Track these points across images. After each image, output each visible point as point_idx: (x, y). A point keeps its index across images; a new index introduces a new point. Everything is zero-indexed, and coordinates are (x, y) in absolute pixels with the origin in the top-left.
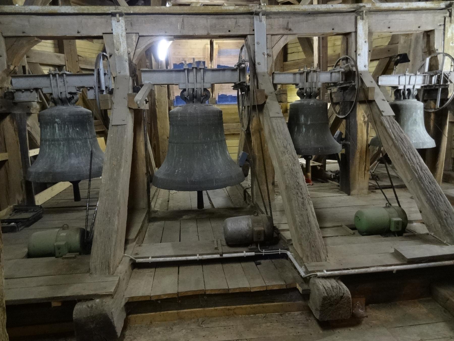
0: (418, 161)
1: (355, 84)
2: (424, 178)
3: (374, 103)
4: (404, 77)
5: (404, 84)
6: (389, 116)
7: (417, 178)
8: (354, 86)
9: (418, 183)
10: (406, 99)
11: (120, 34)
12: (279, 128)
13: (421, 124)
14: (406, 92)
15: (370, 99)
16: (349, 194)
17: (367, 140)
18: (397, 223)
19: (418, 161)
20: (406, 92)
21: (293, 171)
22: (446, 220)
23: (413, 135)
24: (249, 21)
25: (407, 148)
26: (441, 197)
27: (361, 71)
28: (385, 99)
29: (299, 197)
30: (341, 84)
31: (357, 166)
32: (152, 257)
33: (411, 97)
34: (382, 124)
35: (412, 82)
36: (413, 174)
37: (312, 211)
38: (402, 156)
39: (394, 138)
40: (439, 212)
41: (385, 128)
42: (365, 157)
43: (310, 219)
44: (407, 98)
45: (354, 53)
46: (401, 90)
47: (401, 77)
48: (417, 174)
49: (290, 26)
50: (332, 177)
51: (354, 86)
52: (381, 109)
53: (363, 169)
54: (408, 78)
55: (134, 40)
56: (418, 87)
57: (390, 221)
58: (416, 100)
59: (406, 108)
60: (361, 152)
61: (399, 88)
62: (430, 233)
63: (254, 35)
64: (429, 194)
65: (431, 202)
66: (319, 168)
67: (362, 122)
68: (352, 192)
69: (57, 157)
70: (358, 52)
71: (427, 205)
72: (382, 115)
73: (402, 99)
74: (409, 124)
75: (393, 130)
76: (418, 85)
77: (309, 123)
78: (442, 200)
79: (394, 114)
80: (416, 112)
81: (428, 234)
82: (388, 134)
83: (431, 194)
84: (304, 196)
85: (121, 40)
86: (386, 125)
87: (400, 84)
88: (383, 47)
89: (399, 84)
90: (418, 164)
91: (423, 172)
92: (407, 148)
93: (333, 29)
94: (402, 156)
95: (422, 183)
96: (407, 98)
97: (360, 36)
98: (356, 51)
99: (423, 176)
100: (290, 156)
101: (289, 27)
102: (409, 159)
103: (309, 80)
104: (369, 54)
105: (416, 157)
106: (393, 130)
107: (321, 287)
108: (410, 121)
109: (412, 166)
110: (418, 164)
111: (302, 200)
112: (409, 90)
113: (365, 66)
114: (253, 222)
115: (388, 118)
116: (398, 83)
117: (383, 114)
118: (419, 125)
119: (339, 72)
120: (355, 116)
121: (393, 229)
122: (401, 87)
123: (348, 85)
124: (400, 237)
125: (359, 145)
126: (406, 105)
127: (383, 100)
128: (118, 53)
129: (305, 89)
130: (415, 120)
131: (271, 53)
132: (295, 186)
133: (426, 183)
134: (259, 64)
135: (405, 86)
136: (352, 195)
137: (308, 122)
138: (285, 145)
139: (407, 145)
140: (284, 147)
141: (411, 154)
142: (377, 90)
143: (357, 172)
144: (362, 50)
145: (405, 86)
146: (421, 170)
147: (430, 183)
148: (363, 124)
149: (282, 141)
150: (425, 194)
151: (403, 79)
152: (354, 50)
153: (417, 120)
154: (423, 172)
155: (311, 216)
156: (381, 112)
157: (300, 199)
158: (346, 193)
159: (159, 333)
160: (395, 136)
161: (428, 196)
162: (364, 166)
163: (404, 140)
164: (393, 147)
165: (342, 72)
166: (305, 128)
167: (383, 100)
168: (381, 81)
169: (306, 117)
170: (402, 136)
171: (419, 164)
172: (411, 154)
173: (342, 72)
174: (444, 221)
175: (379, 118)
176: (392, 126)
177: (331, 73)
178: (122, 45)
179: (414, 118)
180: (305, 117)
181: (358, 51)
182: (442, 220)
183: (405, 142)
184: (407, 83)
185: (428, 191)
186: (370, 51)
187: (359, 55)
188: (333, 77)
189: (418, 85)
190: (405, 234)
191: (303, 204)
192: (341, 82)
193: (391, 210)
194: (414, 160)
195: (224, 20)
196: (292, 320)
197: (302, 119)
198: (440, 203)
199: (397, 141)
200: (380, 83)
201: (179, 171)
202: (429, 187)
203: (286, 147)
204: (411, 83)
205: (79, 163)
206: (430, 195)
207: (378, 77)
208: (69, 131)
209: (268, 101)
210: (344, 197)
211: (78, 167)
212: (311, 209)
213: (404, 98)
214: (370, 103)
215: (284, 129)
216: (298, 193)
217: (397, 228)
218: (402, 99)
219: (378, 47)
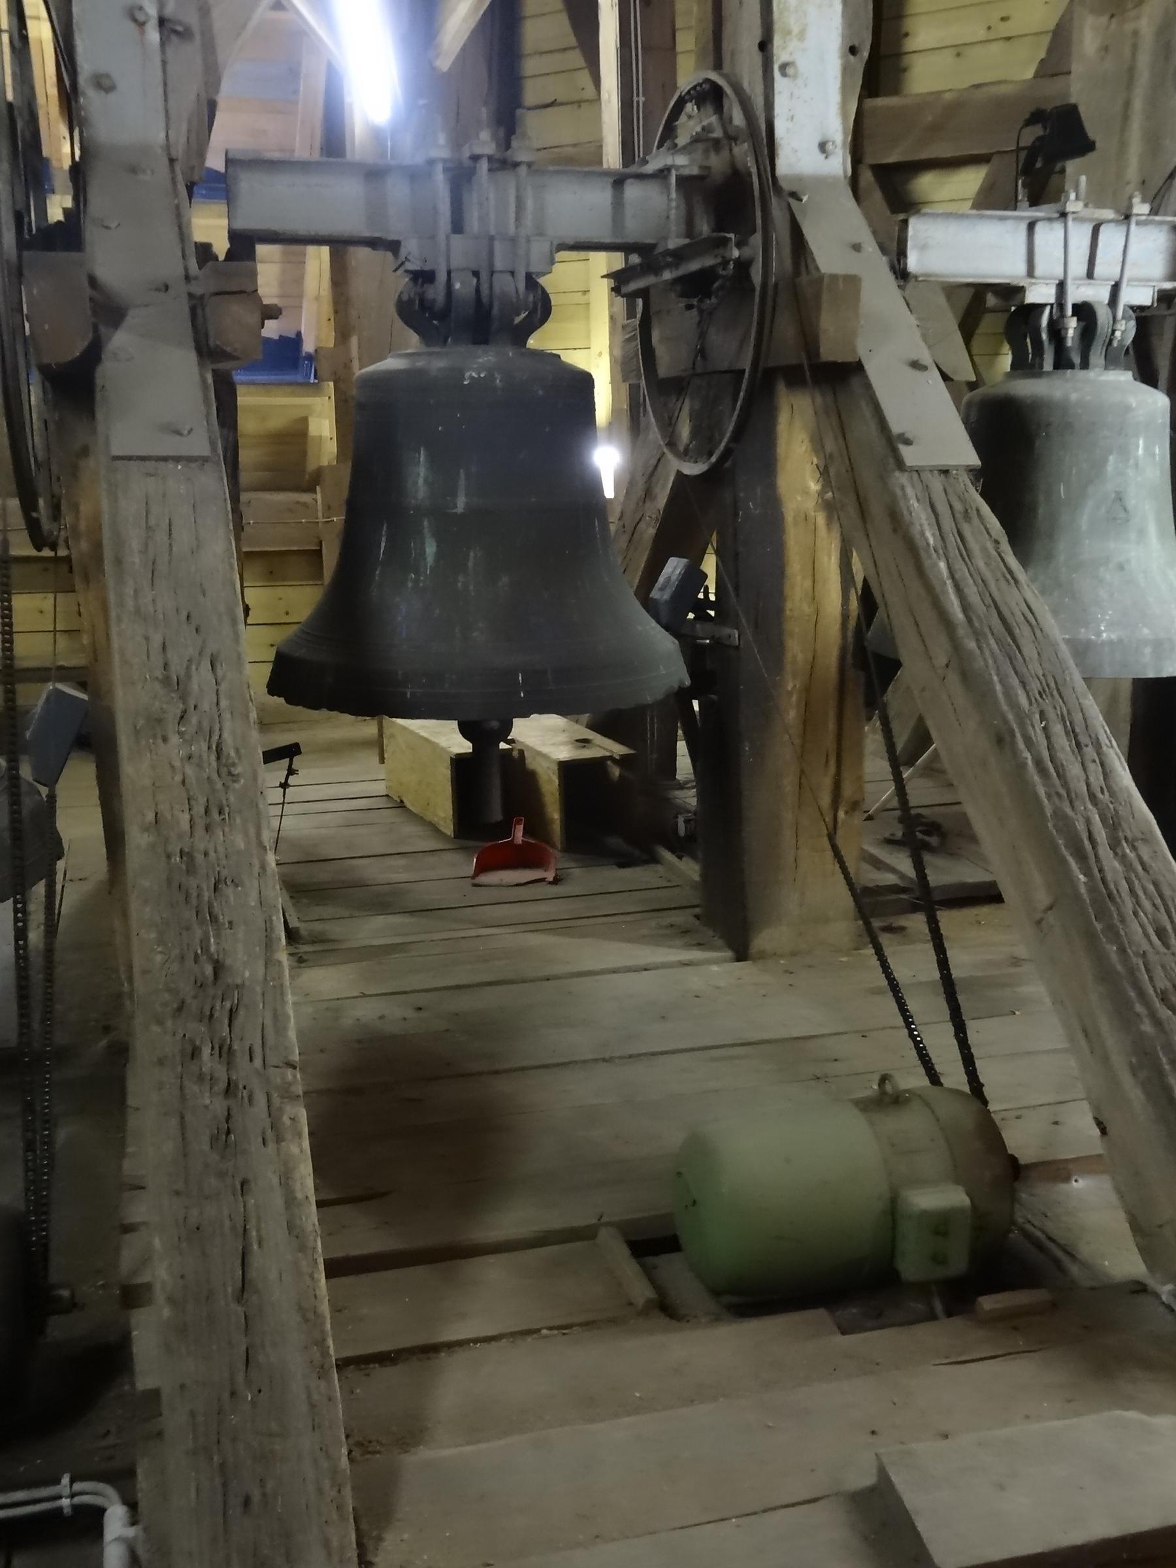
0: (1097, 780)
1: (747, 252)
2: (1129, 905)
3: (855, 382)
4: (1058, 229)
5: (1059, 272)
6: (945, 472)
7: (1077, 896)
8: (743, 266)
9: (1090, 937)
10: (1071, 366)
12: (161, 537)
13: (1152, 529)
14: (1072, 325)
15: (829, 352)
16: (741, 954)
17: (845, 616)
18: (940, 1224)
19: (1097, 780)
20: (1072, 325)
21: (191, 869)
23: (1103, 593)
25: (1035, 686)
27: (799, 179)
28: (926, 358)
29: (201, 1078)
30: (678, 256)
31: (789, 784)
33: (1097, 356)
34: (897, 520)
35: (1107, 266)
37: (291, 1201)
39: (959, 615)
41: (912, 549)
42: (832, 726)
43: (257, 1259)
44: (1077, 360)
45: (757, 57)
46: (1041, 306)
47: (1039, 228)
48: (1087, 873)
50: (682, 830)
51: (743, 266)
52: (896, 428)
53: (826, 800)
54: (1080, 237)
56: (1140, 295)
57: (893, 1210)
58: (1124, 377)
60: (807, 690)
61: (1032, 298)
62: (1152, 1283)
64: (1153, 1015)
66: (616, 772)
67: (810, 504)
68: (762, 941)
70: (782, 52)
71: (1135, 1094)
72: (900, 465)
73: (1048, 364)
74: (1084, 521)
75: (959, 565)
76: (1143, 281)
77: (461, 503)
79: (974, 460)
80: (1125, 452)
81: (1139, 1288)
83: (1164, 1013)
84: (244, 1071)
86: (915, 531)
87: (1038, 271)
88: (1003, 89)
89: (1031, 273)
90: (1093, 797)
91: (1123, 859)
92: (1035, 686)
94: (1002, 740)
95: (1113, 933)
96: (1077, 360)
98: (765, 46)
99: (1124, 885)
102: (1039, 763)
103: (473, 222)
104: (846, 70)
105: (1090, 752)
106: (959, 565)
108: (1090, 504)
109: (1058, 814)
110: (1093, 797)
111: (219, 1106)
112: (1084, 311)
113: (822, 147)
115: (937, 484)
116: (1021, 268)
117: (910, 455)
118: (1142, 533)
119: (662, 174)
120: (768, 465)
121: (911, 1267)
122: (1040, 293)
123: (708, 261)
124: (957, 1322)
125: (796, 650)
126: (1064, 407)
127: (916, 365)
129: (442, 277)
130: (1119, 498)
131: (191, 18)
132: (187, 989)
133: (1136, 932)
135: (1061, 287)
136: (762, 956)
137: (454, 495)
138: (177, 669)
139: (1035, 667)
140: (166, 681)
141: (1058, 729)
142: (879, 292)
143: (788, 816)
144: (802, 36)
145: (1061, 287)
146: (1114, 845)
147: (1161, 933)
148: (821, 519)
149: (157, 640)
150: (1124, 1016)
151: (1049, 237)
152: (757, 35)
153: (1131, 502)
154: (1123, 859)
155: (275, 1231)
156: (893, 441)
157: (212, 1103)
158: (731, 945)
160: (966, 607)
161: (1147, 1027)
162: (827, 782)
164: (953, 678)
165: (683, 181)
167: (916, 365)
168: (923, 248)
170: (1012, 601)
171: (1105, 798)
172: (1058, 729)
173: (683, 181)
175: (883, 478)
176: (952, 539)
177: (619, 182)
179: (1110, 487)
180: (432, 460)
181: (777, 41)
183: (1029, 650)
184: (1078, 266)
185: (1142, 994)
186: (853, 50)
187: (784, 67)
188: (629, 211)
189: (1143, 281)
190: (988, 1303)
191: (225, 1136)
192: (673, 243)
193: (912, 1124)
194: (1074, 769)
197: (419, 478)
199: (978, 636)
200: (913, 262)
202: (1152, 957)
203: (178, 686)
204: (1098, 270)
206: (1158, 1022)
207: (905, 222)
209: (120, 340)
210: (713, 972)
212: (286, 1178)
213: (1063, 362)
214: (840, 378)
215: (197, 548)
217: (938, 1259)
218: (1048, 364)
219: (985, 89)
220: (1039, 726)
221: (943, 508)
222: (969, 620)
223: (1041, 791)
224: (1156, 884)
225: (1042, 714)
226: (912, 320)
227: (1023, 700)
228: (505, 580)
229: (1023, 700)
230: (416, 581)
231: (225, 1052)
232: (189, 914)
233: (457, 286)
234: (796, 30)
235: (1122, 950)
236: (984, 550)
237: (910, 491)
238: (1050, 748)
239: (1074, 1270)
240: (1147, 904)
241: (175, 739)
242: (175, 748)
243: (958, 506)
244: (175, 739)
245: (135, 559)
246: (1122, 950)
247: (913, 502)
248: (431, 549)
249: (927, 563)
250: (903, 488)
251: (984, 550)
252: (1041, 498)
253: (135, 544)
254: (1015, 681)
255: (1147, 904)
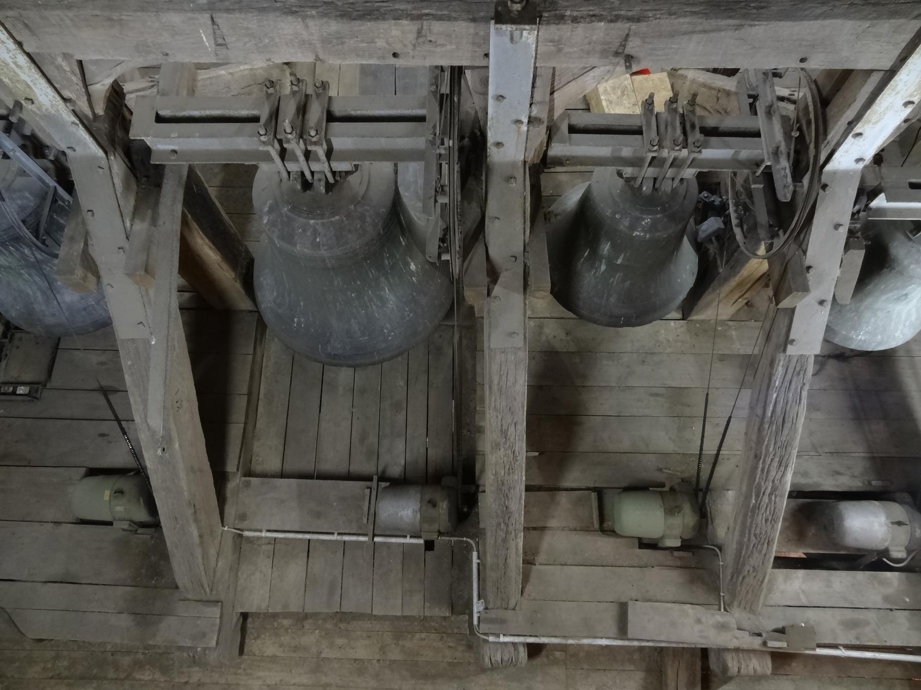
9: (745, 516)
11: (9, 61)
12: (504, 378)
21: (503, 484)
22: (744, 578)
24: (472, 30)
25: (779, 444)
26: (766, 545)
32: (268, 531)
36: (748, 498)
37: (517, 549)
38: (756, 456)
40: (743, 565)
43: (508, 560)
48: (756, 501)
49: (633, 47)
55: (67, 69)
59: (901, 273)
63: (487, 67)
65: (741, 549)
69: (30, 292)
72: (785, 350)
77: (619, 261)
78: (764, 551)
82: (765, 402)
83: (753, 538)
85: (23, 77)
86: (774, 378)
90: (773, 481)
93: (803, 60)
95: (753, 517)
97: (901, 86)
98: (851, 124)
100: (509, 452)
101: (629, 50)
104: (899, 127)
105: (782, 468)
107: (487, 660)
109: (759, 484)
114: (423, 520)
128: (39, 109)
130: (906, 295)
134: (499, 144)
138: (505, 427)
139: (784, 438)
141: (777, 459)
147: (766, 520)
149: (500, 417)
150: (742, 534)
152: (850, 119)
154: (770, 499)
155: (513, 556)
159: (286, 631)
160: (774, 411)
161: (745, 540)
163: (788, 425)
166: (607, 265)
169: (616, 249)
174: (741, 578)
176: (786, 384)
178: (36, 90)
180: (612, 246)
182: (738, 577)
183: (786, 432)
191: (505, 540)
194: (773, 473)
195: (369, 25)
196: (456, 631)
198: (756, 555)
199: (771, 423)
201: (299, 323)
203: (504, 433)
205: (82, 298)
206: (749, 539)
208: (23, 253)
211: (85, 309)
216: (500, 524)
220: (771, 457)
221: (790, 371)
222: (772, 416)
223: (758, 476)
224: (775, 508)
225: (774, 455)
226: (837, 272)
227: (771, 449)
228: (629, 282)
229: (771, 449)
230: (595, 274)
231: (507, 525)
232: (502, 496)
233: (644, 189)
234: (873, 121)
235: (752, 522)
236: (796, 388)
237: (781, 363)
238: (770, 465)
239: (710, 527)
240: (768, 513)
241: (502, 450)
242: (502, 452)
243: (798, 369)
244: (502, 450)
245: (495, 387)
246: (752, 522)
247: (780, 368)
248: (603, 268)
249: (770, 392)
250: (780, 361)
251: (796, 388)
252: (873, 284)
253: (496, 382)
254: (773, 443)
255: (768, 513)
